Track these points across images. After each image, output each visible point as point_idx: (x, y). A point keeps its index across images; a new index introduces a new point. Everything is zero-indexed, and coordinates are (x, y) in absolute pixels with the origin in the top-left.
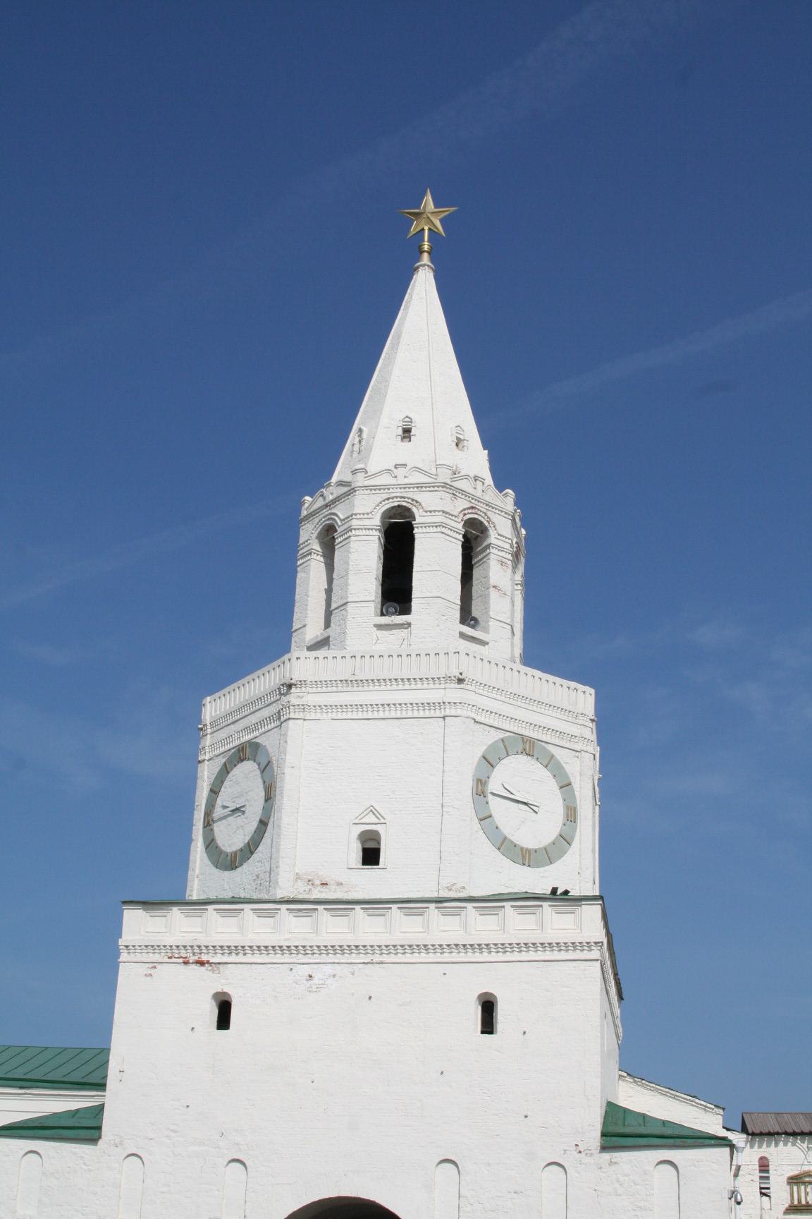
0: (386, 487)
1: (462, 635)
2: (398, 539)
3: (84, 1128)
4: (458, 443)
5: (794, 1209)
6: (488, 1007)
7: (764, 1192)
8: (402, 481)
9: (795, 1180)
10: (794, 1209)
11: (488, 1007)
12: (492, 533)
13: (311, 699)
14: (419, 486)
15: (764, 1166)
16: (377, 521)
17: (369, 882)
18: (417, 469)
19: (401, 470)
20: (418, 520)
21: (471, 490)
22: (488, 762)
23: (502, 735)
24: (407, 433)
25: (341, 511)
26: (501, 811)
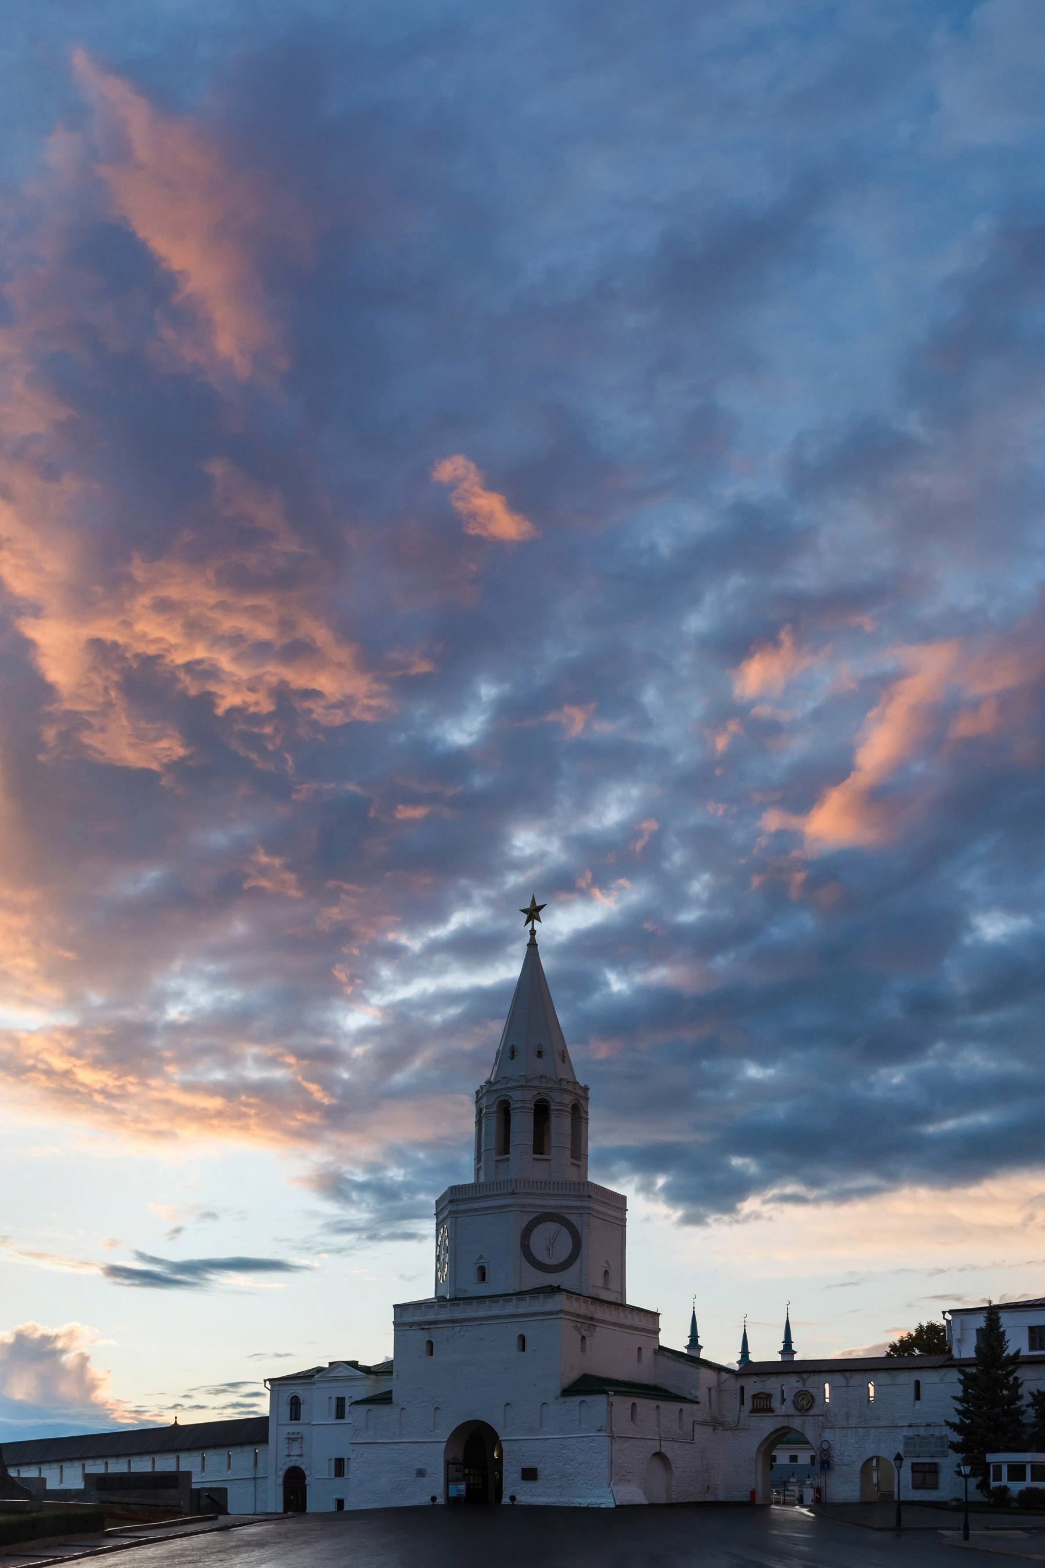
0: (499, 1090)
3: (384, 1399)
4: (540, 1054)
5: (754, 1410)
6: (522, 1338)
7: (742, 1403)
9: (754, 1397)
10: (754, 1410)
11: (522, 1338)
12: (552, 1103)
14: (511, 1088)
15: (742, 1388)
18: (510, 1079)
20: (512, 1106)
23: (534, 1215)
24: (513, 1052)
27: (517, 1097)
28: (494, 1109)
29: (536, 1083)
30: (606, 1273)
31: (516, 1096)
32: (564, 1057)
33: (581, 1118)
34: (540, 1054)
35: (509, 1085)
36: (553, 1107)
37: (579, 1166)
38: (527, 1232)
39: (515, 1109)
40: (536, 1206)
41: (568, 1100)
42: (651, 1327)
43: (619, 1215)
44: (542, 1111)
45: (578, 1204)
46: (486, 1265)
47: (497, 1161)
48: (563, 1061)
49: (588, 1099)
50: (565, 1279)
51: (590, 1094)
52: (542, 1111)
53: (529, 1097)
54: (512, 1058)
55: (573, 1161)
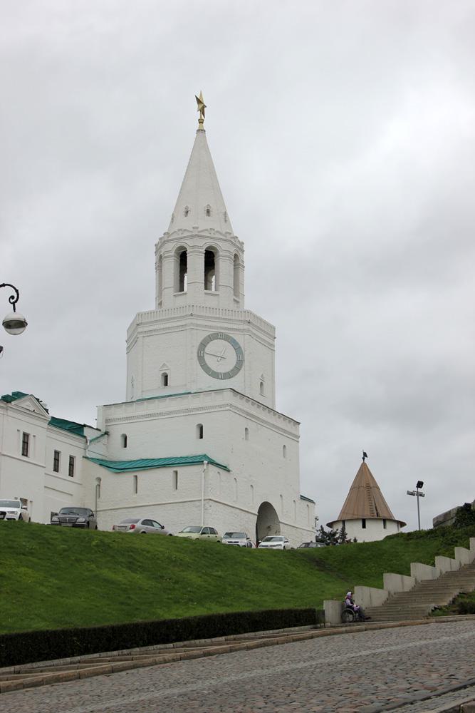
0: (177, 239)
1: (206, 294)
2: (183, 258)
4: (208, 212)
8: (181, 236)
11: (201, 428)
13: (145, 329)
14: (188, 237)
16: (173, 254)
17: (167, 391)
18: (185, 230)
19: (181, 232)
21: (209, 235)
22: (203, 345)
25: (163, 250)
26: (210, 361)
27: (188, 244)
30: (261, 384)
32: (226, 217)
33: (239, 264)
34: (208, 212)
36: (221, 253)
37: (238, 302)
39: (191, 252)
41: (233, 250)
42: (293, 432)
43: (270, 341)
44: (210, 259)
45: (241, 327)
46: (167, 372)
49: (243, 251)
50: (233, 383)
52: (210, 259)
55: (235, 297)
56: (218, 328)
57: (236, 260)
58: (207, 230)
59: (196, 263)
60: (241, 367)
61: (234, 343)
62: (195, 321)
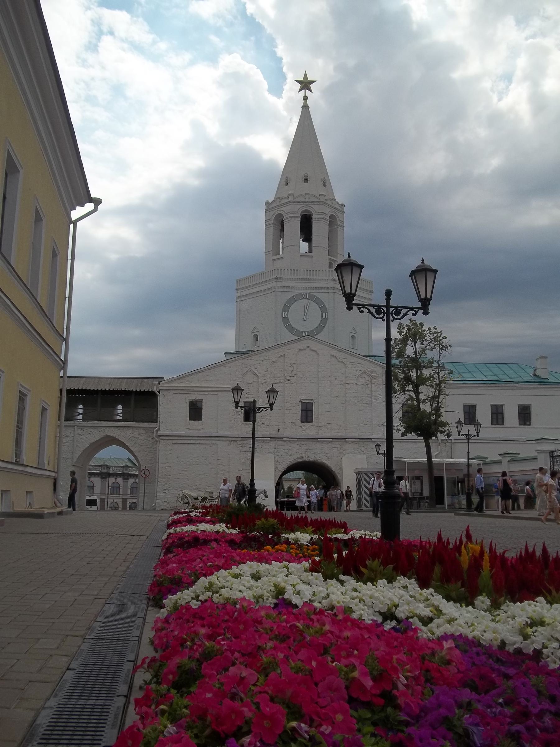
4: (306, 181)
18: (283, 198)
21: (304, 200)
23: (293, 294)
28: (272, 222)
29: (301, 199)
31: (286, 209)
34: (306, 181)
35: (282, 202)
36: (314, 216)
38: (286, 308)
40: (292, 287)
47: (274, 260)
48: (324, 185)
51: (345, 209)
53: (298, 210)
54: (287, 184)
56: (300, 288)
57: (333, 223)
58: (302, 195)
59: (293, 227)
60: (325, 325)
61: (318, 302)
62: (279, 284)
